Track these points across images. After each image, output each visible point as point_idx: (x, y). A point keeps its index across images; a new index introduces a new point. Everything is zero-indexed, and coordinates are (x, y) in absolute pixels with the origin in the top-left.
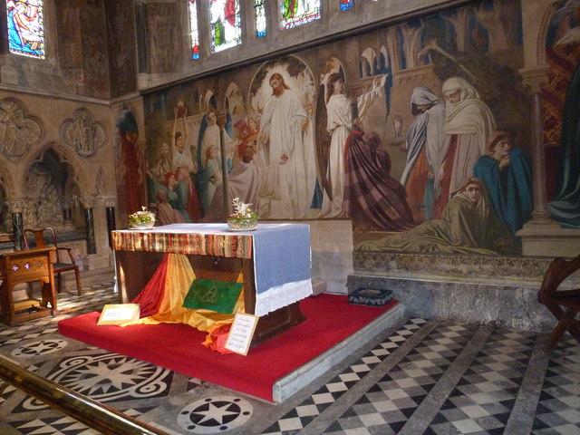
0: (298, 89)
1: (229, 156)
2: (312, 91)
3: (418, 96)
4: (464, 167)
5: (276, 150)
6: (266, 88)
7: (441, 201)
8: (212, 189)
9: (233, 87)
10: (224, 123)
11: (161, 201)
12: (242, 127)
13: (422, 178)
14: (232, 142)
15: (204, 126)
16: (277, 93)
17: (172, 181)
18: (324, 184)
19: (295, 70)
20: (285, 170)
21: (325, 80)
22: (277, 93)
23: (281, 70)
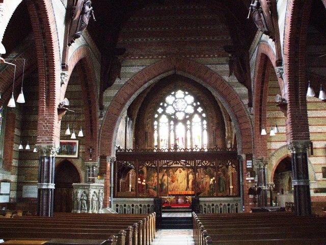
0: (184, 173)
1: (169, 181)
2: (187, 173)
3: (202, 176)
4: (208, 186)
5: (179, 181)
6: (178, 171)
7: (205, 190)
8: (164, 187)
9: (171, 170)
10: (168, 175)
11: (150, 188)
12: (173, 177)
13: (203, 188)
14: (170, 179)
15: (163, 175)
16: (180, 172)
17: (154, 185)
18: (188, 187)
19: (184, 170)
20: (181, 185)
21: (189, 172)
22: (180, 172)
23: (181, 169)
